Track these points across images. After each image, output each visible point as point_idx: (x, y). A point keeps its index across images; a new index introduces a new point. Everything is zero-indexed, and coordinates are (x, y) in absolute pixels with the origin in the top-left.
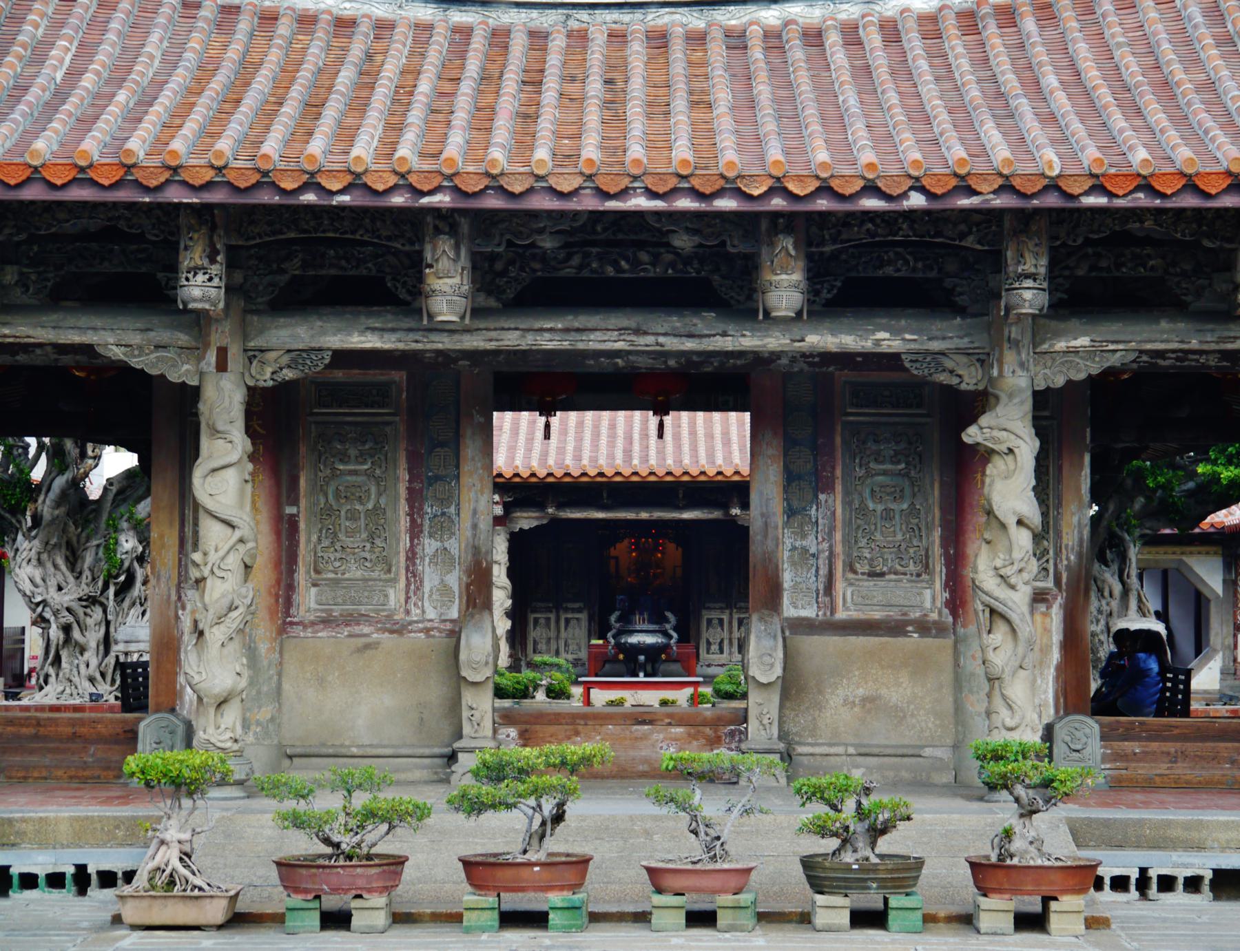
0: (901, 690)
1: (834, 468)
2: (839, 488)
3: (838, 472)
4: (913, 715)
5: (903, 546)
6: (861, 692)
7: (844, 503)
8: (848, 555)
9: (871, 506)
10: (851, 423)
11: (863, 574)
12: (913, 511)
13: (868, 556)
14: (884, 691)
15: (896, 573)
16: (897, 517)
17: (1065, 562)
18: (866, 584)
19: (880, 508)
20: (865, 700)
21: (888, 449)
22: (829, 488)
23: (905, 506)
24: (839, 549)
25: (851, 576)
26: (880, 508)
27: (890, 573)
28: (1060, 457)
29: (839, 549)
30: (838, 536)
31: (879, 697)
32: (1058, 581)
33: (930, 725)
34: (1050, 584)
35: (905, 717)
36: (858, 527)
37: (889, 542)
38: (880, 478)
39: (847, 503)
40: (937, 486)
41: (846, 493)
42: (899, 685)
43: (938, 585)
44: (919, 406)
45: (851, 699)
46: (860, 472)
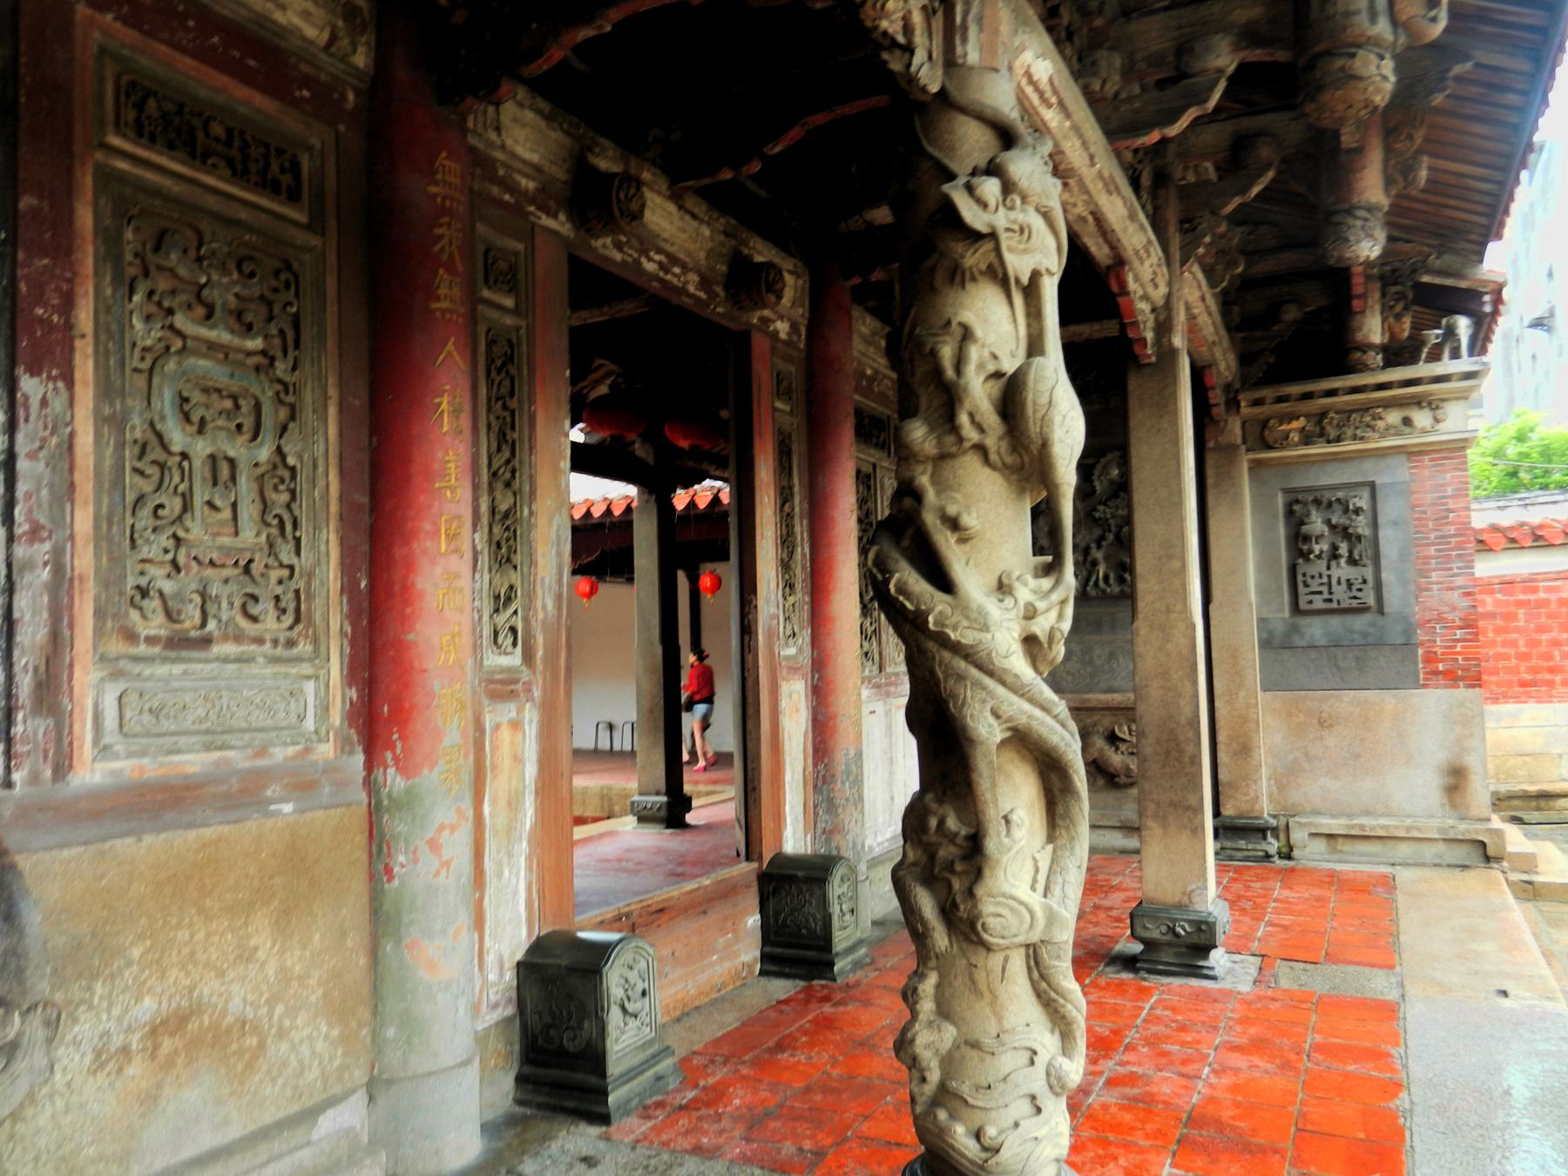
0: (253, 970)
1: (68, 304)
2: (85, 367)
3: (84, 317)
4: (282, 1034)
5: (256, 568)
6: (148, 1007)
7: (100, 420)
8: (109, 581)
9: (178, 437)
10: (122, 178)
11: (151, 640)
12: (282, 471)
13: (168, 586)
14: (209, 988)
15: (238, 638)
16: (243, 480)
17: (541, 616)
18: (161, 670)
19: (201, 448)
20: (155, 1031)
21: (225, 290)
22: (54, 358)
23: (264, 453)
24: (84, 561)
25: (115, 646)
26: (201, 448)
27: (225, 638)
28: (531, 402)
29: (84, 561)
30: (83, 520)
31: (196, 1009)
32: (528, 657)
33: (320, 1046)
34: (514, 659)
35: (262, 1045)
36: (140, 500)
37: (227, 551)
38: (202, 364)
39: (111, 422)
40: (332, 411)
41: (107, 390)
42: (246, 955)
43: (335, 669)
44: (294, 196)
45: (117, 1042)
46: (144, 333)
